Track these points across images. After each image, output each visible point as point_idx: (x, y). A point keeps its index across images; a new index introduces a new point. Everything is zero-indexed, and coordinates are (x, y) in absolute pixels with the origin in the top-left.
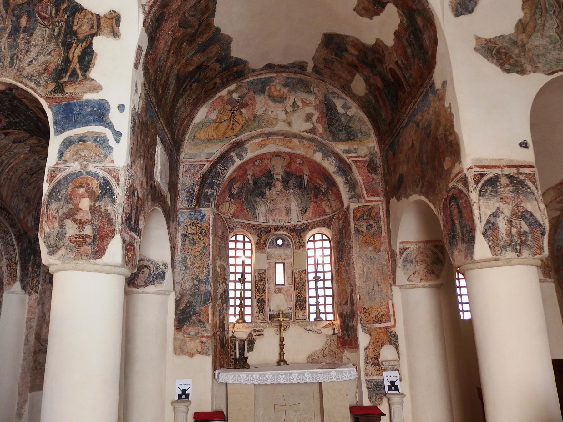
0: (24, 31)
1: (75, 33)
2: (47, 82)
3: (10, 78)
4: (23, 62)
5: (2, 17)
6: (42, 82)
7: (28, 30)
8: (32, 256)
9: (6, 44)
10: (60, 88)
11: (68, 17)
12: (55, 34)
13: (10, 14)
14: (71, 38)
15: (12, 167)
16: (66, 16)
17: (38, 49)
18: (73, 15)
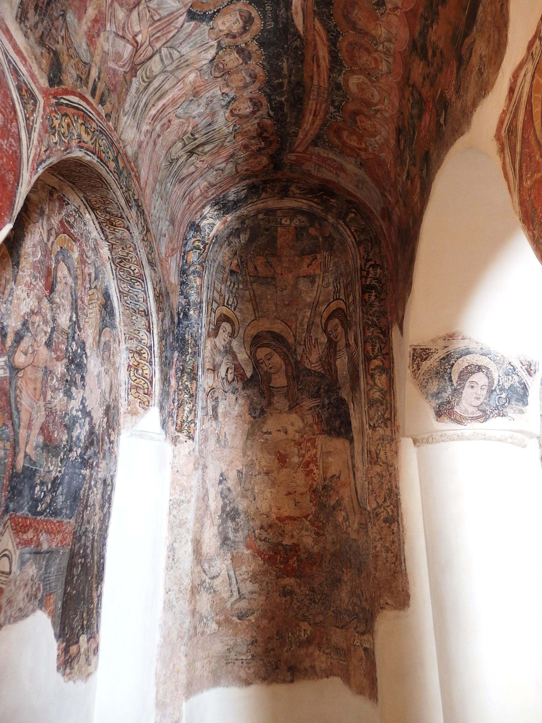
8: (176, 354)
15: (164, 107)
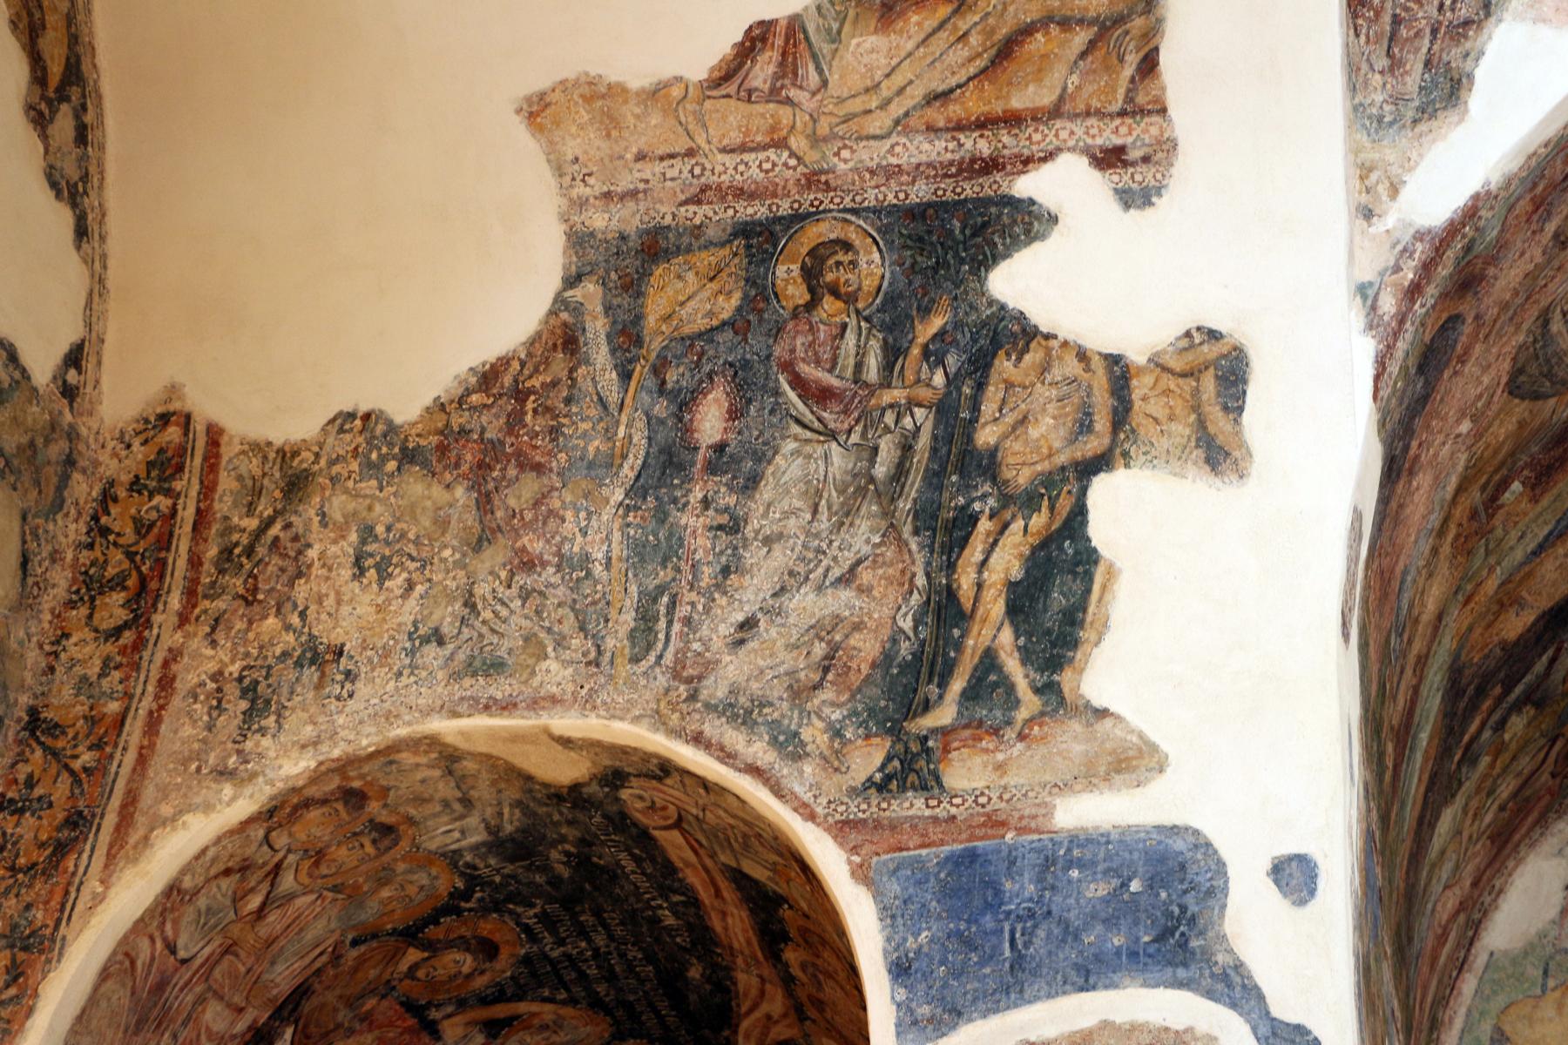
0: (712, 468)
1: (989, 465)
2: (838, 734)
3: (636, 720)
4: (705, 631)
5: (601, 401)
6: (814, 735)
7: (736, 460)
9: (617, 536)
10: (912, 768)
11: (952, 381)
12: (880, 471)
13: (641, 387)
14: (966, 487)
16: (939, 379)
17: (781, 557)
18: (979, 367)
